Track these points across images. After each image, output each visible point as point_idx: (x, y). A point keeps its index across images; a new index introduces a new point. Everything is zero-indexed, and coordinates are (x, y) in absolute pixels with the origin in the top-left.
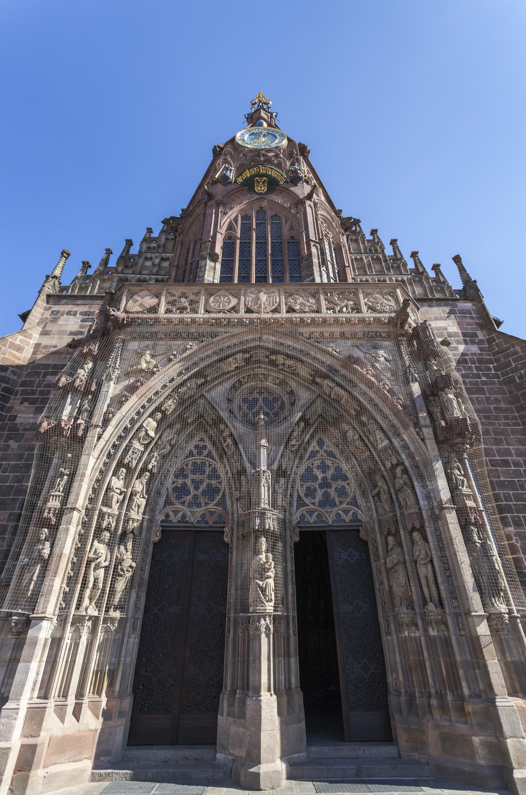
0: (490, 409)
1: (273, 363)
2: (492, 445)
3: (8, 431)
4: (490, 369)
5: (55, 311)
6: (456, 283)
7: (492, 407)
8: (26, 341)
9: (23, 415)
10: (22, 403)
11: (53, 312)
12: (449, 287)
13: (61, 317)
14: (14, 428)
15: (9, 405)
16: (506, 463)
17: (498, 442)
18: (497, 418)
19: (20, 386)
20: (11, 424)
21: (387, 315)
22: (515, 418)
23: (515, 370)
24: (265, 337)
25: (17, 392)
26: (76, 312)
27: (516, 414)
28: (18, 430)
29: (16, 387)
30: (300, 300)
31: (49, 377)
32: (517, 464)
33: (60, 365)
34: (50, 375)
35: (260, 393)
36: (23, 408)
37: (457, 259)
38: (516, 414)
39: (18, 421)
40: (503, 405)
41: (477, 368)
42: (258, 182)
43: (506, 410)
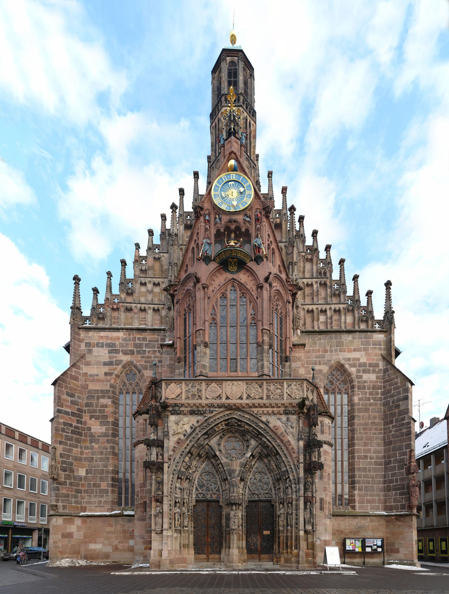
0: (368, 423)
2: (362, 446)
3: (89, 437)
4: (378, 394)
5: (88, 343)
6: (379, 314)
8: (78, 371)
9: (94, 427)
10: (90, 419)
11: (86, 343)
12: (373, 317)
13: (93, 349)
14: (92, 436)
15: (83, 420)
17: (366, 444)
18: (371, 429)
19: (86, 407)
20: (89, 433)
22: (381, 429)
25: (85, 411)
26: (102, 343)
28: (95, 437)
29: (83, 407)
31: (101, 400)
32: (371, 458)
33: (104, 390)
34: (100, 398)
36: (93, 423)
37: (388, 284)
38: (382, 427)
39: (93, 431)
40: (377, 421)
41: (371, 394)
42: (231, 263)
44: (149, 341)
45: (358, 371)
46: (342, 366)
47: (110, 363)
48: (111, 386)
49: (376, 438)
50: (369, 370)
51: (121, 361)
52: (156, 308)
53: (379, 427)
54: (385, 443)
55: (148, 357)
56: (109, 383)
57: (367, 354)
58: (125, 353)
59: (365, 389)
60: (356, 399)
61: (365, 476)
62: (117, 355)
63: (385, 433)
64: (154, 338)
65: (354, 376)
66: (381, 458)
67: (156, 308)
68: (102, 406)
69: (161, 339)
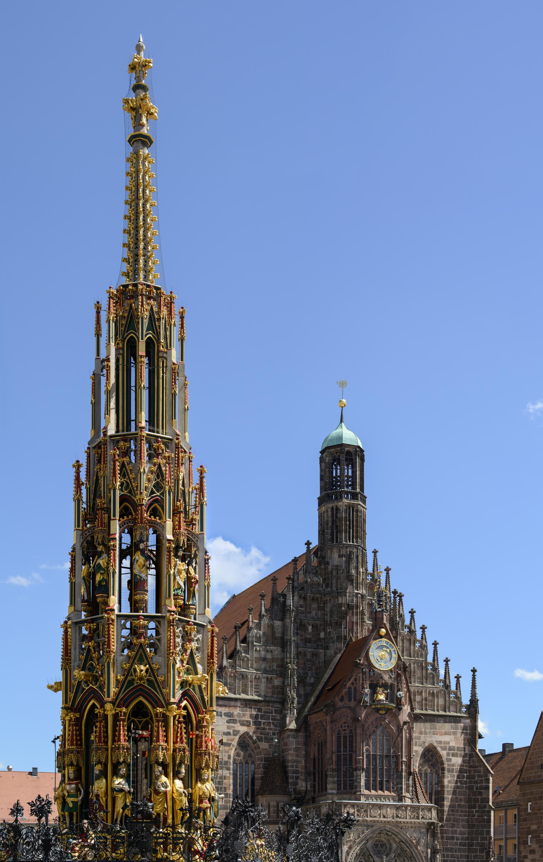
1: (387, 834)
4: (463, 777)
7: (457, 804)
16: (453, 838)
17: (453, 826)
18: (457, 811)
21: (427, 821)
22: (466, 812)
23: (476, 782)
24: (387, 826)
27: (467, 809)
30: (401, 812)
35: (379, 842)
37: (474, 671)
38: (467, 809)
40: (463, 803)
41: (458, 777)
43: (464, 806)
44: (264, 712)
45: (448, 754)
46: (435, 748)
47: (229, 734)
48: (229, 757)
49: (462, 820)
50: (457, 754)
51: (238, 731)
52: (269, 678)
53: (464, 809)
54: (469, 825)
55: (263, 729)
56: (227, 754)
57: (456, 739)
58: (242, 724)
59: (453, 772)
60: (446, 781)
61: (452, 856)
62: (235, 725)
63: (469, 816)
64: (269, 709)
65: (444, 759)
66: (466, 840)
67: (269, 678)
68: (221, 778)
69: (275, 710)
